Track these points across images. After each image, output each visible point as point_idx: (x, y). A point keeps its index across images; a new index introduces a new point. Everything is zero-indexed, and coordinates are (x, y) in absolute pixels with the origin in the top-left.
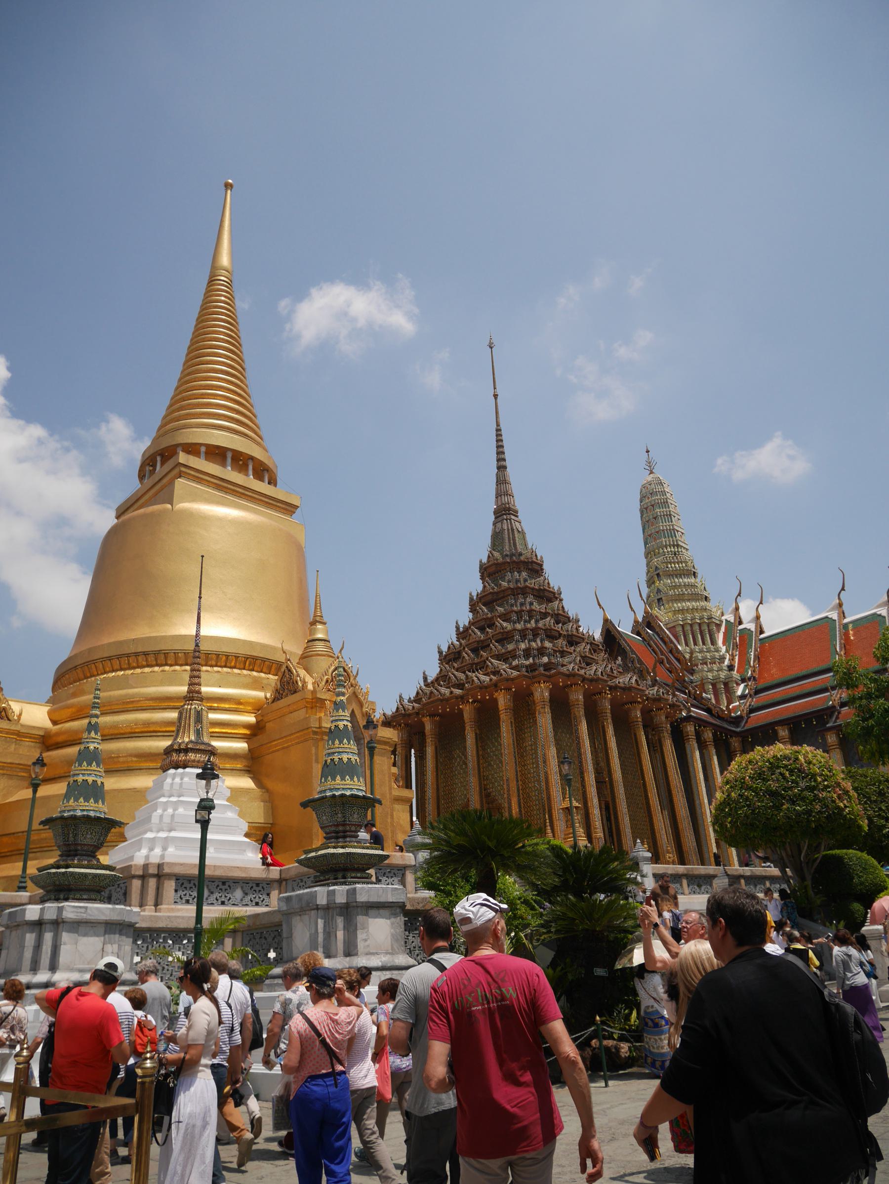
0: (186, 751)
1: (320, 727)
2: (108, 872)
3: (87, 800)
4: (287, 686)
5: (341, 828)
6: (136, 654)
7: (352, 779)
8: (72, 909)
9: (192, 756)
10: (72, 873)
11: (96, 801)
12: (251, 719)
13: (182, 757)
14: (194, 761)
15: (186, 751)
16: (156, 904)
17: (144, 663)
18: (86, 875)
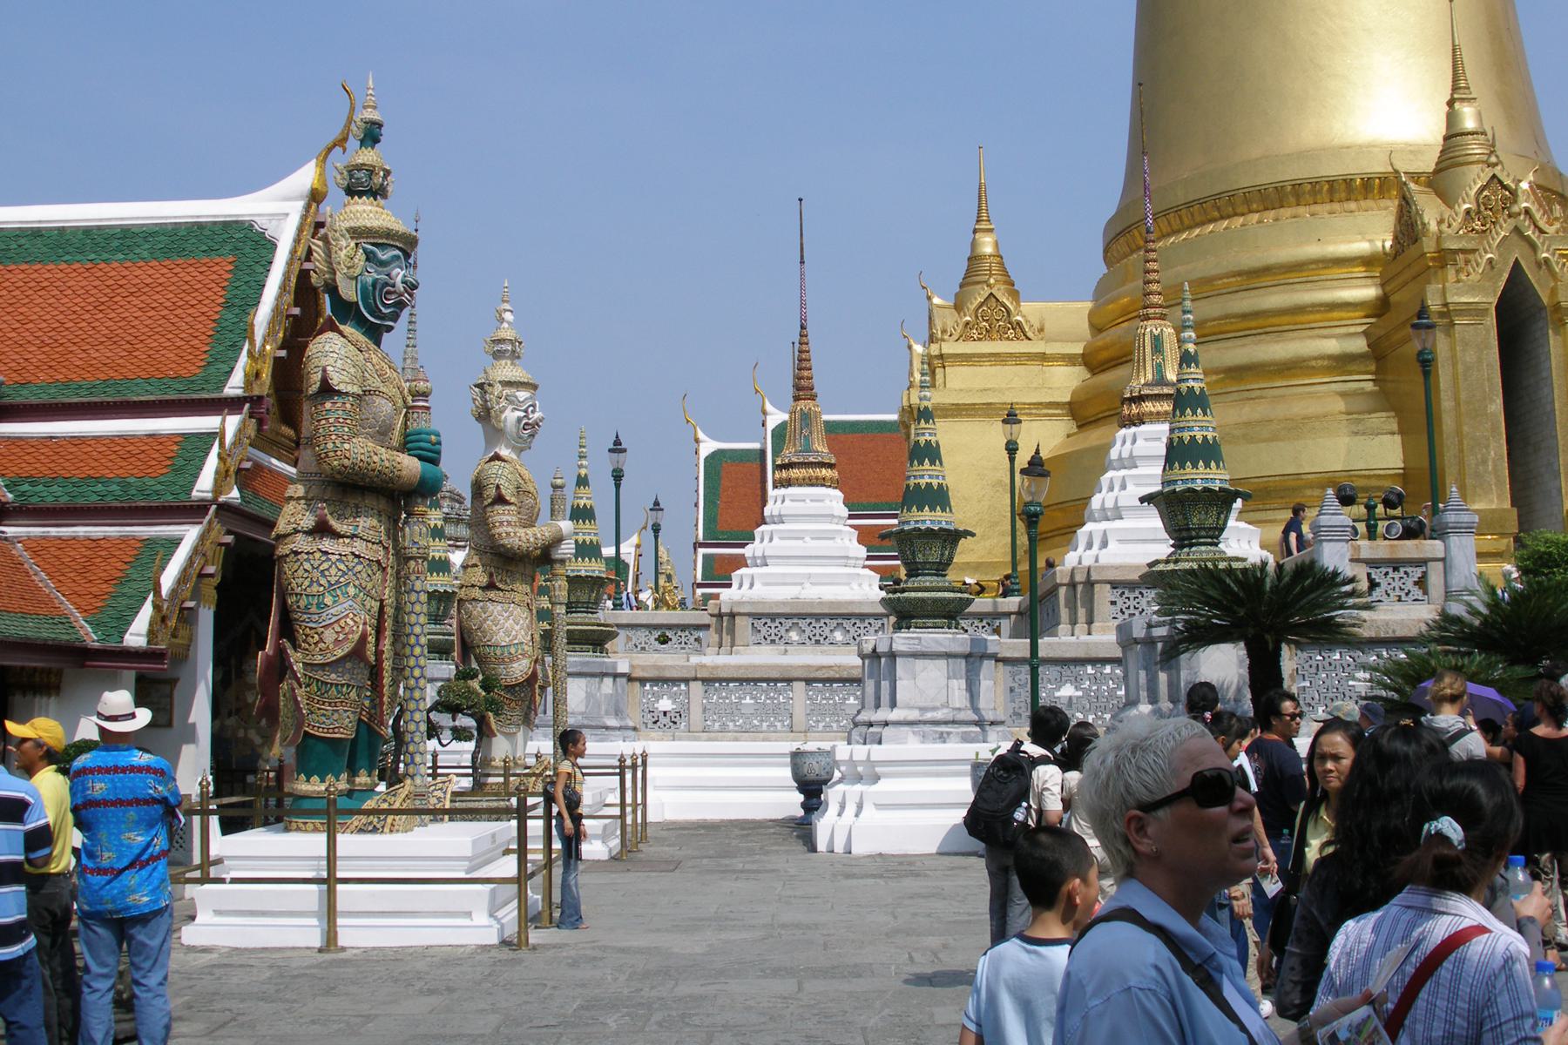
0: (1141, 399)
1: (1446, 305)
2: (951, 595)
3: (920, 509)
4: (1408, 228)
5: (1185, 534)
6: (1189, 205)
7: (1195, 466)
8: (903, 641)
9: (1148, 407)
10: (906, 599)
11: (932, 509)
12: (1369, 292)
13: (1135, 409)
14: (1151, 413)
15: (1141, 399)
16: (1090, 622)
17: (1216, 214)
18: (923, 600)
